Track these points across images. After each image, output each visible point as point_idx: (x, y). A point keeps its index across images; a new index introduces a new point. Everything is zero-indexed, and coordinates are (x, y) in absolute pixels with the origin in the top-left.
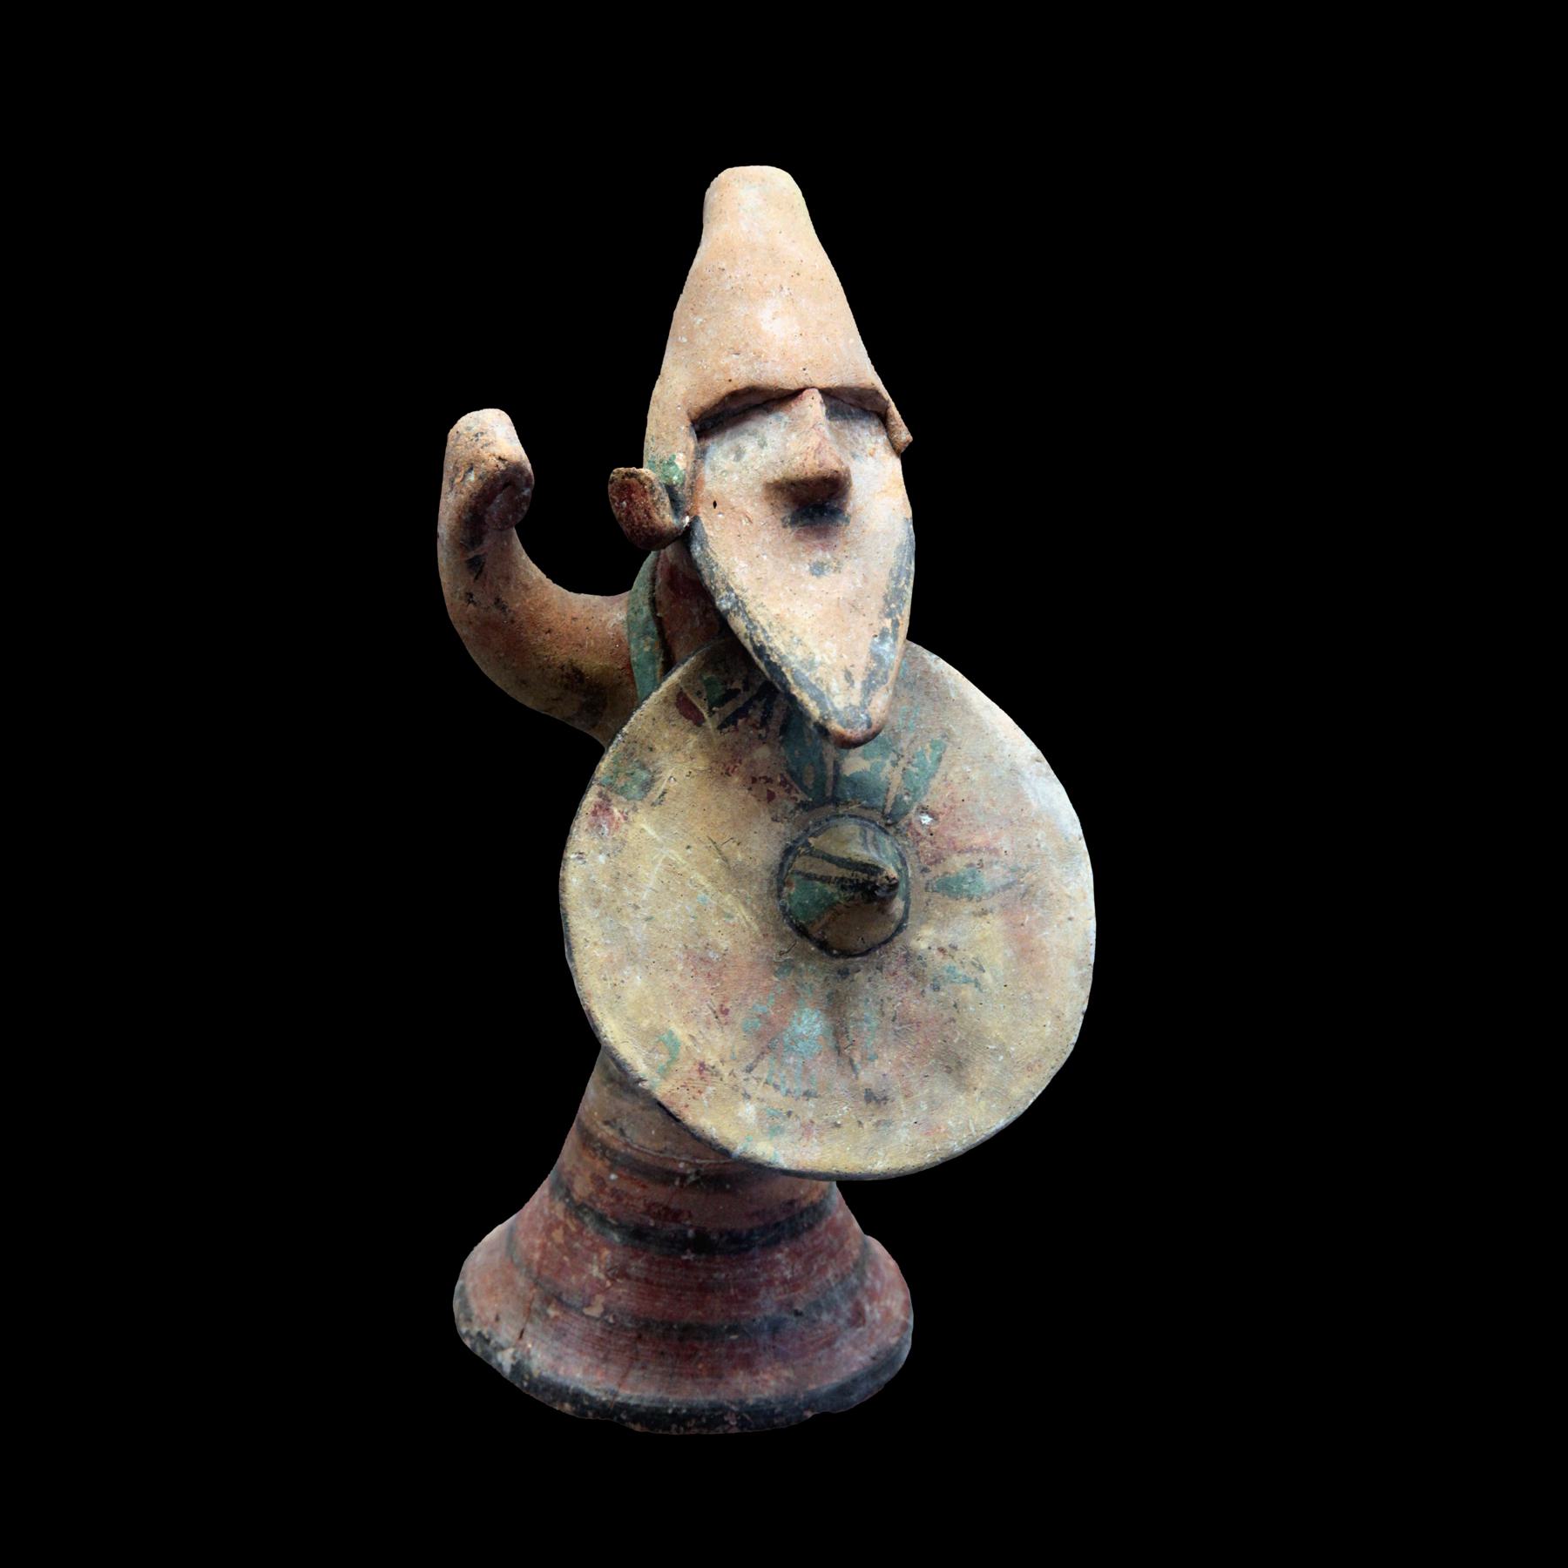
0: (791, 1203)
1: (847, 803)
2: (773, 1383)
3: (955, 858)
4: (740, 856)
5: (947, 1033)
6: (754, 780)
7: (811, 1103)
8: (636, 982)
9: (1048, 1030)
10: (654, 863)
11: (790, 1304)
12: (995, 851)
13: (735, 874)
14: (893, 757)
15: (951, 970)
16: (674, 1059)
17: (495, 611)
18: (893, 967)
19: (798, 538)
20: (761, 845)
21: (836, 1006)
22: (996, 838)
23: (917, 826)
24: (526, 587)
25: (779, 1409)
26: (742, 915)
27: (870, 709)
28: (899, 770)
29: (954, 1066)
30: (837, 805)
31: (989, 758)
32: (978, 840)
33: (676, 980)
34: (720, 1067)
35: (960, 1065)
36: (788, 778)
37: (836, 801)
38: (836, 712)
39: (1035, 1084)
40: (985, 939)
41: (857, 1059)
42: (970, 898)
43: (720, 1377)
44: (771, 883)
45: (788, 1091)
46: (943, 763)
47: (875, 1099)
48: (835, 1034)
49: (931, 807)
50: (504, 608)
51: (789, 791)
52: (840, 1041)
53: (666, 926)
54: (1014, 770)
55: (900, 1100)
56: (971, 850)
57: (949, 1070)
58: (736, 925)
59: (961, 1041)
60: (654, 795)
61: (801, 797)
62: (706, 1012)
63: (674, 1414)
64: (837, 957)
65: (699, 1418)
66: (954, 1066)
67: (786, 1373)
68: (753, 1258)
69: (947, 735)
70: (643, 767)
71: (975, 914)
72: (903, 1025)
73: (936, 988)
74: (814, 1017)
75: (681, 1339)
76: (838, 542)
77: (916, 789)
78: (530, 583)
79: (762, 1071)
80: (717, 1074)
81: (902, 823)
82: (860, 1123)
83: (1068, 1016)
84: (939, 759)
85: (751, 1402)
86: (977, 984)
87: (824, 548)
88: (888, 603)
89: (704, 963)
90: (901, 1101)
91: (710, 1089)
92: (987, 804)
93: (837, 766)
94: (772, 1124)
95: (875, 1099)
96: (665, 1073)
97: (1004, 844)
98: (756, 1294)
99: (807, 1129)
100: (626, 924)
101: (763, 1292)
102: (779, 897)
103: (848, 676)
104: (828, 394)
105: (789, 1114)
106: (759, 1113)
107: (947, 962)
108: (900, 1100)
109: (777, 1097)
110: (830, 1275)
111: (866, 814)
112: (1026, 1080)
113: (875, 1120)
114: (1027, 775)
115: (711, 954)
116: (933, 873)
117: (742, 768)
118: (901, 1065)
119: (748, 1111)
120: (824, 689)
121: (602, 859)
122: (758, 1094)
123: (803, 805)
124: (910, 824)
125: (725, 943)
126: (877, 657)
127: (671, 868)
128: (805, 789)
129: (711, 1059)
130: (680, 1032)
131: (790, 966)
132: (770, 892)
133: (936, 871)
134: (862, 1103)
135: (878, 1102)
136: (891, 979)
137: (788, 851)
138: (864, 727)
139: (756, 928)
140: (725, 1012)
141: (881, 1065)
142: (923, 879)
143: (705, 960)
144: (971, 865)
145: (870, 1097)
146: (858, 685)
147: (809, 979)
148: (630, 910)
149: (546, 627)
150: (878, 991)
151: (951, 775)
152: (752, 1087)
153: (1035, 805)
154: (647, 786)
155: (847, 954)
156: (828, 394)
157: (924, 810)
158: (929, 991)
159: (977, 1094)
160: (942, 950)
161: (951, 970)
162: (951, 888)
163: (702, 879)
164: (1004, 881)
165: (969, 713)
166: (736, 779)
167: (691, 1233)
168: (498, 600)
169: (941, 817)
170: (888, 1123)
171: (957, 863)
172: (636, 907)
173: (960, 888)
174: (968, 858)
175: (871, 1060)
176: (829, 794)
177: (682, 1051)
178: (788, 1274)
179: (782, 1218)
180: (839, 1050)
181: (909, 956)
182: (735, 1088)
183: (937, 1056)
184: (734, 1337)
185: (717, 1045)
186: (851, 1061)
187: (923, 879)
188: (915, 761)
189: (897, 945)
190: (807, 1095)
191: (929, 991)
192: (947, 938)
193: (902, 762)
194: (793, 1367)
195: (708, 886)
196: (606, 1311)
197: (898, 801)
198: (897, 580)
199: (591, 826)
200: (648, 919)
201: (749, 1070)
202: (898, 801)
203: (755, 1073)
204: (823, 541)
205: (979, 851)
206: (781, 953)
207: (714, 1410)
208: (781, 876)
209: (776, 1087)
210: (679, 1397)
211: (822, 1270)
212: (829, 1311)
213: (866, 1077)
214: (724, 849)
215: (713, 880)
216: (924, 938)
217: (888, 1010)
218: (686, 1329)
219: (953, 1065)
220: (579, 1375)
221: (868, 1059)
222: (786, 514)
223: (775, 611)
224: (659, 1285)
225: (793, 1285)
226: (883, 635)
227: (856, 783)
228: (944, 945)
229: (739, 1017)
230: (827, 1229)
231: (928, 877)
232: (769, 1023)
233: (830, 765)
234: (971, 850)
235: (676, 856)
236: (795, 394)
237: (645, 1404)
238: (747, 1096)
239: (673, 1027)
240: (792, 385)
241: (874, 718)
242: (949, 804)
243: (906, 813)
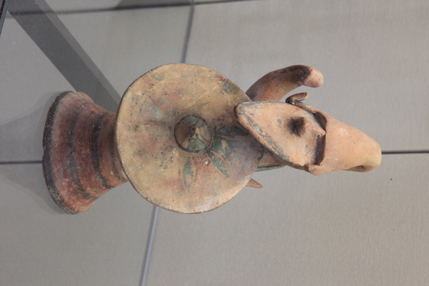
0: (102, 156)
1: (214, 139)
2: (55, 140)
3: (195, 168)
4: (205, 108)
5: (150, 153)
6: (224, 116)
7: (138, 110)
8: (177, 76)
9: (145, 184)
10: (206, 87)
11: (75, 151)
12: (195, 181)
13: (200, 106)
14: (225, 157)
15: (166, 159)
16: (156, 79)
17: (272, 77)
18: (170, 142)
19: (288, 119)
20: (206, 114)
21: (162, 123)
22: (199, 183)
23: (205, 159)
24: (277, 85)
25: (48, 139)
26: (190, 105)
27: (243, 115)
28: (221, 158)
29: (140, 153)
30: (214, 137)
31: (220, 187)
32: (199, 177)
33: (176, 85)
34: (152, 89)
35: (140, 155)
36: (223, 125)
37: (215, 137)
38: (244, 107)
39: (131, 175)
40: (172, 171)
41: (148, 126)
42: (184, 170)
43: (60, 127)
44: (197, 114)
45: (142, 105)
46: (221, 172)
47: (136, 128)
48: (155, 122)
49: (210, 165)
50: (273, 79)
51: (220, 125)
52: (152, 122)
53: (190, 86)
54: (216, 194)
55: (135, 134)
56: (197, 174)
57: (139, 152)
58: (187, 102)
59: (147, 157)
60: (223, 92)
61: (218, 128)
62: (166, 90)
63: (53, 113)
64: (175, 127)
65: (51, 118)
66: (140, 153)
67: (57, 145)
68: (89, 142)
69: (228, 176)
70: (231, 91)
71: (180, 170)
72: (154, 141)
73: (162, 153)
74: (160, 117)
75: (72, 120)
76: (286, 129)
77: (215, 161)
78: (278, 87)
79: (149, 100)
80: (150, 88)
81: (207, 154)
82: (131, 122)
83: (147, 192)
84: (222, 171)
85: (52, 132)
86: (161, 166)
87: (285, 125)
88: (269, 137)
89: (179, 92)
90: (135, 134)
91: (147, 85)
92: (208, 183)
93: (225, 139)
94: (135, 99)
95: (136, 128)
96: (153, 76)
97: (197, 185)
98: (80, 141)
99: (132, 107)
100: (192, 77)
101: (80, 143)
102: (193, 116)
103: (252, 114)
104: (325, 136)
105: (137, 104)
106: (139, 96)
107: (168, 158)
108: (135, 134)
109: (142, 101)
110: (79, 167)
111: (211, 144)
112: (133, 173)
113: (131, 126)
114: (214, 198)
115: (181, 95)
116: (192, 161)
117: (227, 114)
118: (144, 137)
119: (140, 93)
120: (250, 107)
121: (209, 76)
122: (143, 97)
123: (216, 128)
124: (206, 157)
125: (183, 98)
126: (256, 125)
127: (204, 91)
128: (219, 129)
129: (154, 88)
130: (162, 82)
131: (174, 114)
132: (194, 113)
133: (193, 162)
134: (136, 124)
135: (135, 128)
136: (167, 141)
137: (204, 121)
138: (239, 112)
139: (186, 108)
140: (166, 94)
141: (145, 132)
142: (191, 157)
143: (179, 93)
144: (193, 173)
145: (137, 127)
146: (250, 116)
147: (170, 118)
148: (195, 78)
149: (266, 90)
150: (164, 137)
151: (217, 174)
152: (145, 97)
153: (206, 198)
154: (226, 90)
155: (175, 130)
156: (324, 137)
157: (209, 162)
158: (161, 151)
159: (132, 157)
160: (172, 158)
161: (166, 159)
162: (187, 165)
163: (200, 97)
164: (187, 181)
165: (233, 185)
166: (225, 112)
167: (100, 127)
168: (275, 77)
169: (206, 167)
170: (129, 129)
171: (194, 169)
172: (196, 80)
173: (187, 167)
174: (195, 172)
175: (146, 130)
176: (217, 135)
177: (158, 81)
178: (83, 152)
179: (98, 152)
180: (151, 121)
181: (172, 147)
182: (146, 92)
183: (144, 149)
184: (70, 133)
185: (158, 90)
186: (147, 124)
187: (191, 157)
188: (222, 164)
189: (175, 144)
190: (141, 110)
191: (161, 151)
192: (175, 160)
193: (222, 159)
194: (58, 147)
195: (198, 98)
196: (82, 108)
197: (213, 154)
198: (274, 144)
199: (218, 75)
200: (192, 82)
201: (150, 97)
202: (213, 154)
203: (149, 98)
204: (286, 125)
205: (196, 176)
206: (178, 113)
207: (52, 122)
208: (199, 117)
209: (144, 102)
210: (57, 116)
211: (81, 165)
212: (70, 164)
213: (142, 127)
214: (207, 105)
215: (200, 100)
216: (176, 153)
217: (158, 138)
218: (74, 122)
219: (141, 153)
220: (68, 99)
221: (147, 129)
222: (294, 118)
223: (270, 107)
224: (87, 119)
225: (80, 153)
226: (261, 130)
227: (219, 143)
228: (173, 159)
229: (164, 97)
230: (91, 170)
231: (192, 159)
232: (161, 104)
233: (225, 137)
234: (197, 174)
235: (207, 93)
236: (324, 129)
237: (57, 108)
238: (143, 94)
239: (164, 81)
240: (327, 128)
241: (241, 116)
242: (210, 171)
243: (209, 156)
